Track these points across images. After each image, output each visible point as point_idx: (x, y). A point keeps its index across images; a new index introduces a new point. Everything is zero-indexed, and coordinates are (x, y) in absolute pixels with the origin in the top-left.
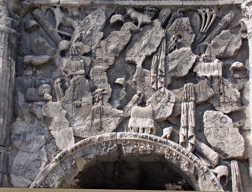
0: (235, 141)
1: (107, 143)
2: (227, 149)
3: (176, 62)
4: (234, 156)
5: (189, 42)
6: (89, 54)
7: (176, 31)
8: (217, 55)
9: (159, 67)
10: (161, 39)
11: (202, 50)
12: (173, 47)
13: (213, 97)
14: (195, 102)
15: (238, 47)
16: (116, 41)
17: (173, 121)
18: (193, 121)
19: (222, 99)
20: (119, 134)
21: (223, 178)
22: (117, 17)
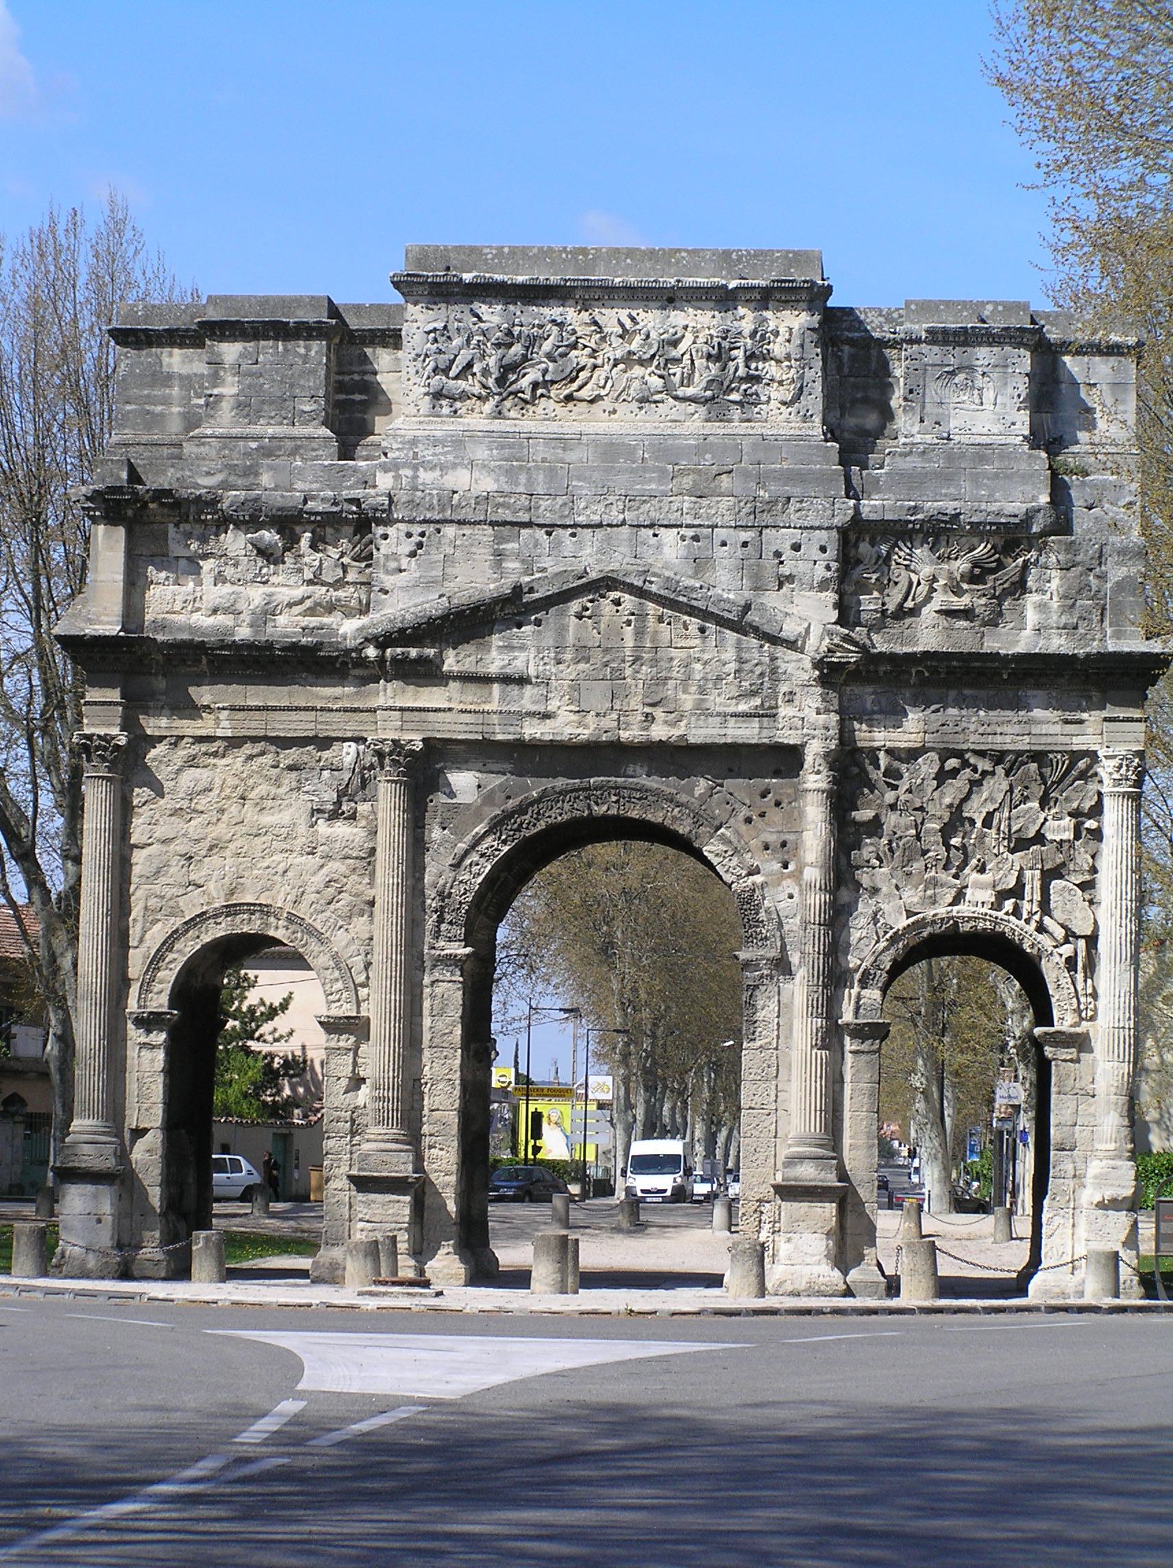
1: (942, 919)
6: (921, 809)
7: (1021, 780)
11: (1052, 804)
13: (1063, 864)
14: (1042, 870)
16: (952, 792)
17: (1017, 892)
19: (1072, 867)
20: (955, 908)
21: (1068, 960)
22: (952, 763)
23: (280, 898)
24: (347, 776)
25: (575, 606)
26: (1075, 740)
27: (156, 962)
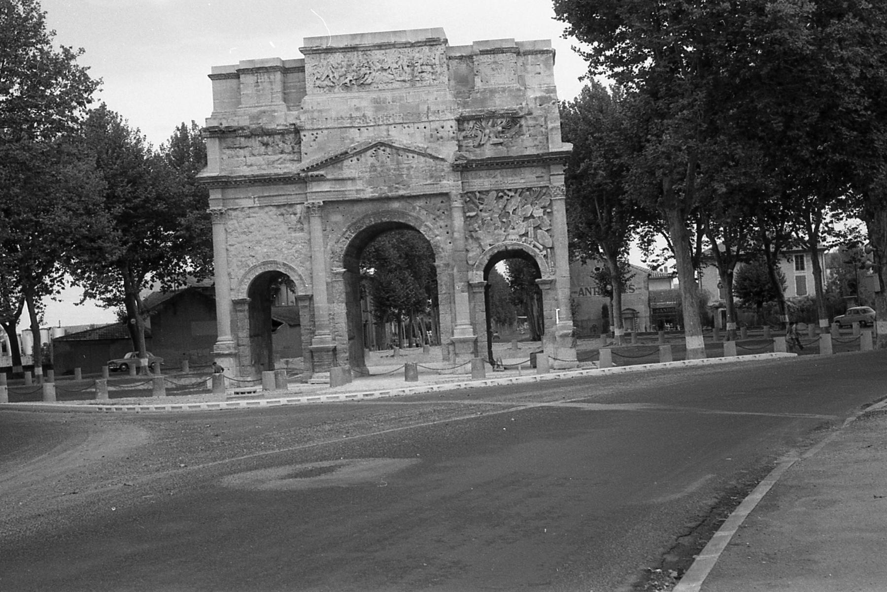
22: (501, 194)
23: (279, 259)
24: (298, 215)
25: (370, 152)
27: (241, 282)
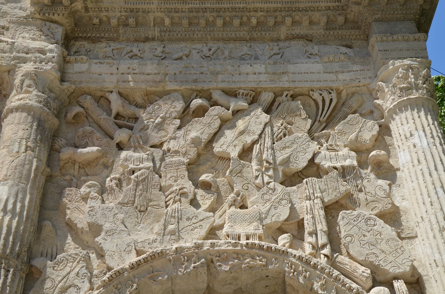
0: (394, 249)
2: (384, 262)
3: (288, 151)
4: (398, 271)
5: (303, 129)
8: (346, 143)
9: (264, 156)
10: (263, 124)
12: (282, 134)
13: (349, 195)
15: (375, 132)
16: (198, 130)
18: (324, 224)
26: (341, 76)
